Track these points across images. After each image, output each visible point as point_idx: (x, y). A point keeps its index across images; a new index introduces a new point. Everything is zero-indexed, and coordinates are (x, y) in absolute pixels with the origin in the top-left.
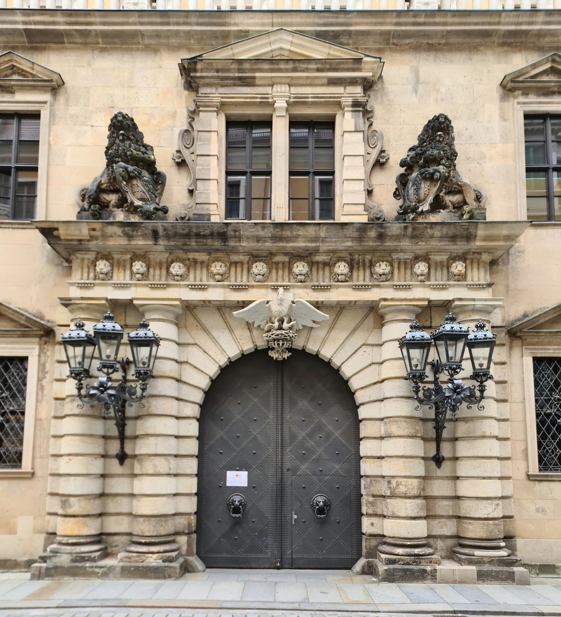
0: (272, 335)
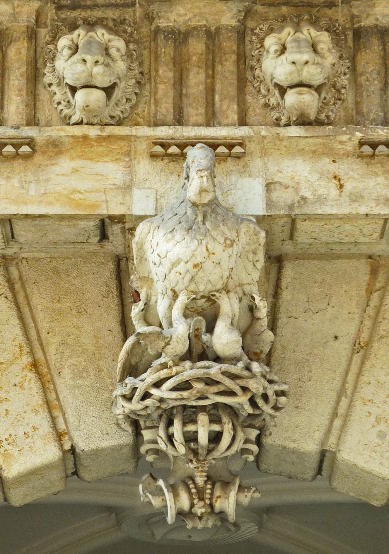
0: (158, 385)
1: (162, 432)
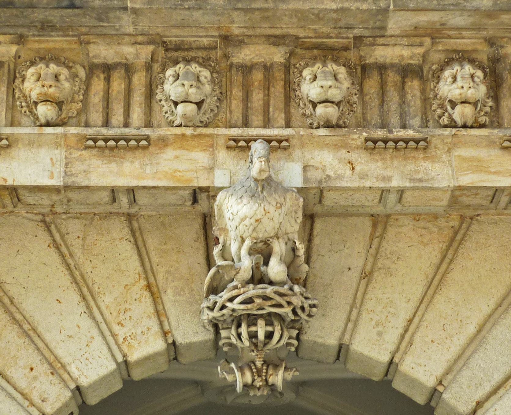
0: (231, 300)
1: (233, 331)
